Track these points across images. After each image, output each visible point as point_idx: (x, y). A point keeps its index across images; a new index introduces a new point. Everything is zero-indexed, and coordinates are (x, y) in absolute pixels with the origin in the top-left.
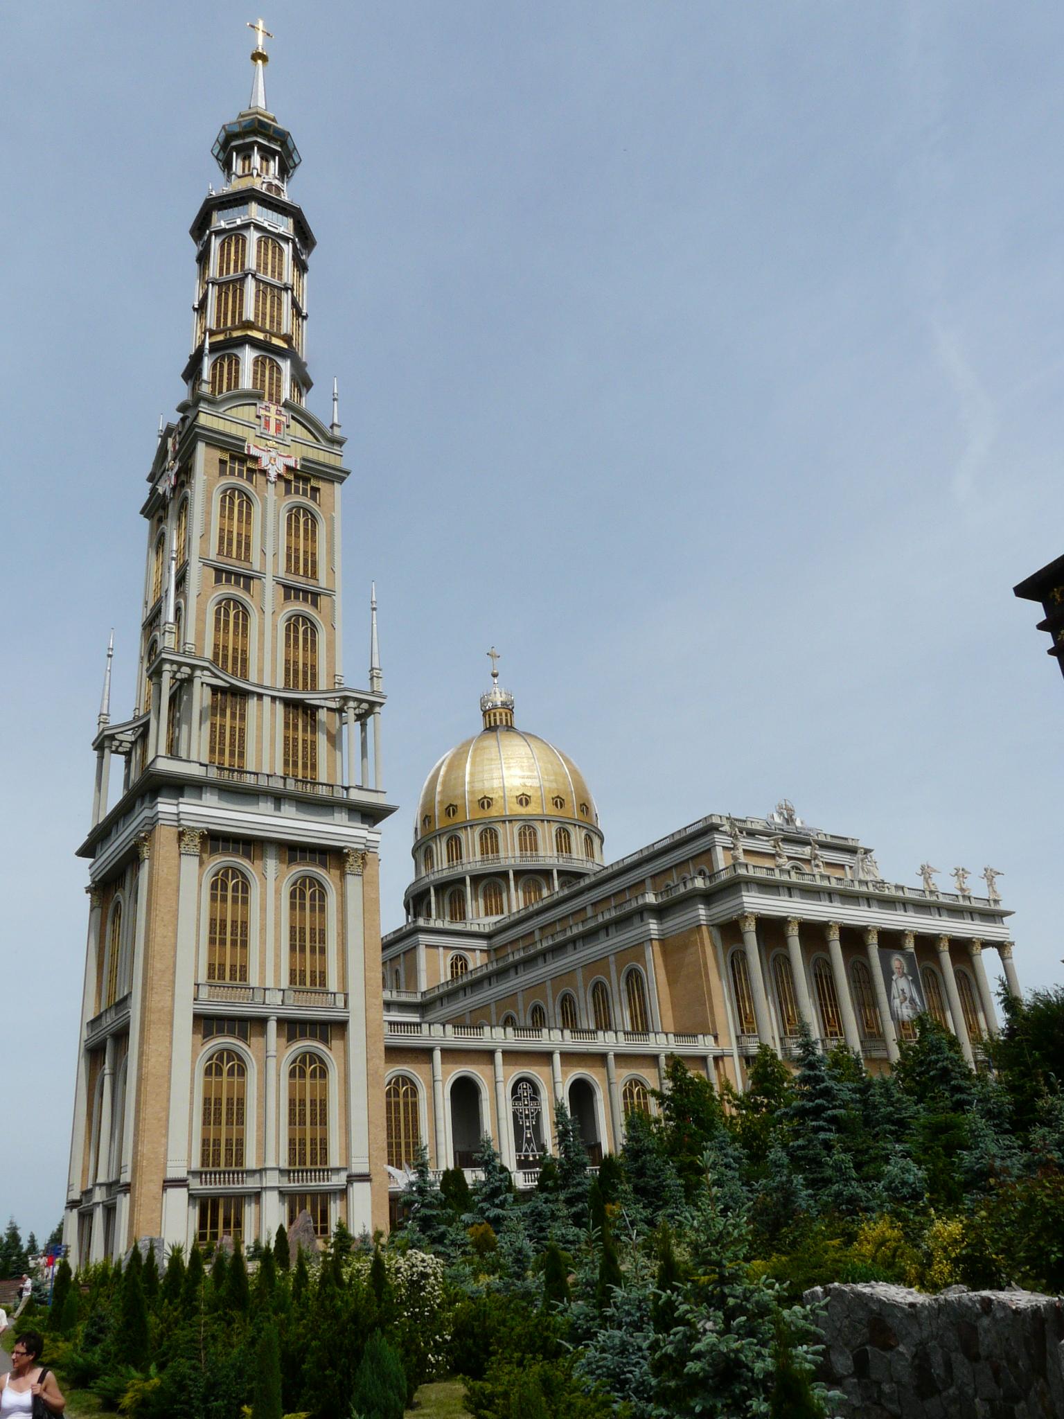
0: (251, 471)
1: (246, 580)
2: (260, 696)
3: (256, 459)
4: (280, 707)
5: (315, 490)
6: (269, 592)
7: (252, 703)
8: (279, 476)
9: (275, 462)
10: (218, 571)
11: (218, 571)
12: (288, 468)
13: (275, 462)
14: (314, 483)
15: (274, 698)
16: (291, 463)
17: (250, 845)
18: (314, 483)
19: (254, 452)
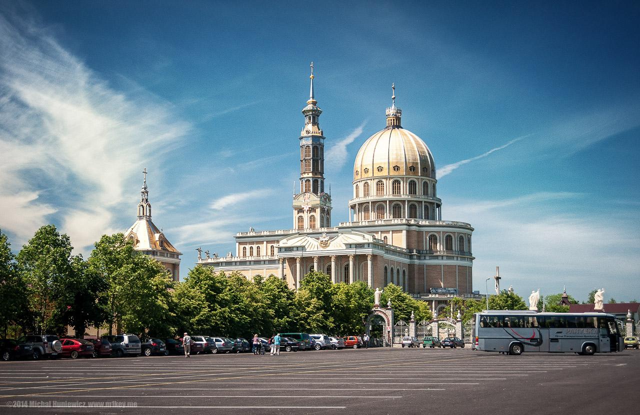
5: (315, 210)
9: (306, 208)
13: (306, 208)
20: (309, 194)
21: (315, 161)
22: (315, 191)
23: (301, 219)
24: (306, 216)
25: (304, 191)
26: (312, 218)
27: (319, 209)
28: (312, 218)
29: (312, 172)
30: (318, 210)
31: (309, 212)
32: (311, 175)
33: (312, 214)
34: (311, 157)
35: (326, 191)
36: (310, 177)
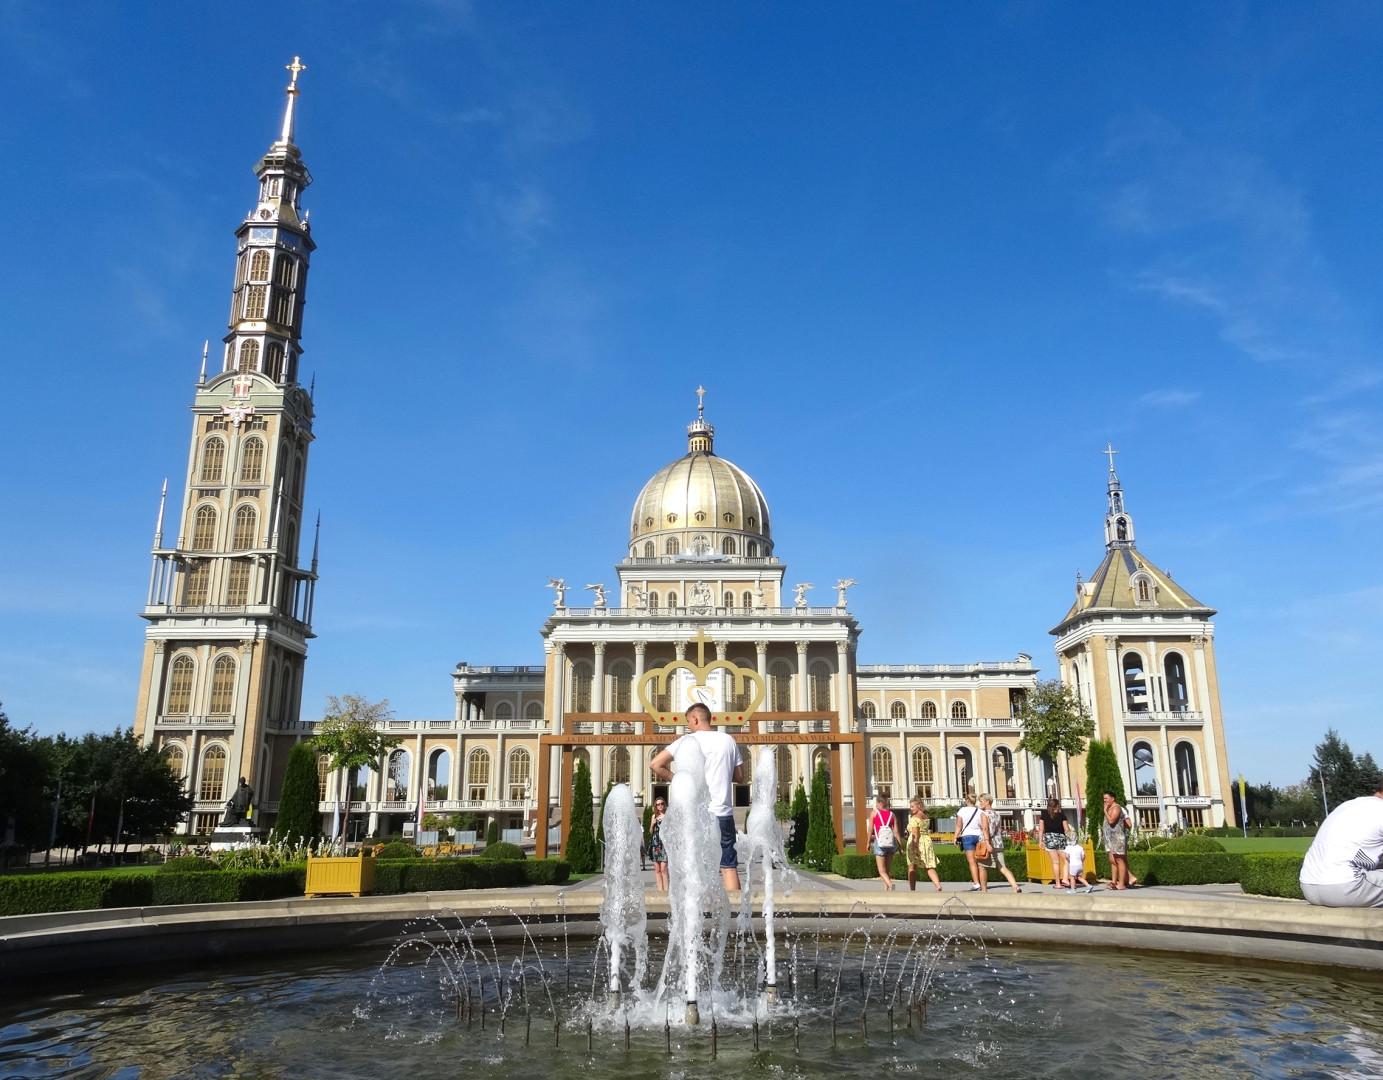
0: (227, 422)
1: (217, 493)
2: (217, 558)
3: (227, 415)
4: (228, 561)
6: (226, 495)
7: (213, 561)
8: (241, 422)
10: (201, 491)
11: (201, 491)
12: (247, 415)
13: (236, 414)
14: (265, 418)
15: (225, 558)
16: (249, 411)
17: (195, 643)
18: (265, 418)
19: (226, 411)
20: (251, 377)
21: (279, 292)
22: (270, 370)
23: (214, 447)
24: (232, 441)
25: (236, 366)
26: (253, 447)
27: (279, 416)
28: (253, 447)
29: (267, 321)
30: (275, 423)
31: (244, 425)
32: (262, 326)
33: (253, 433)
34: (269, 279)
35: (303, 381)
36: (258, 334)
